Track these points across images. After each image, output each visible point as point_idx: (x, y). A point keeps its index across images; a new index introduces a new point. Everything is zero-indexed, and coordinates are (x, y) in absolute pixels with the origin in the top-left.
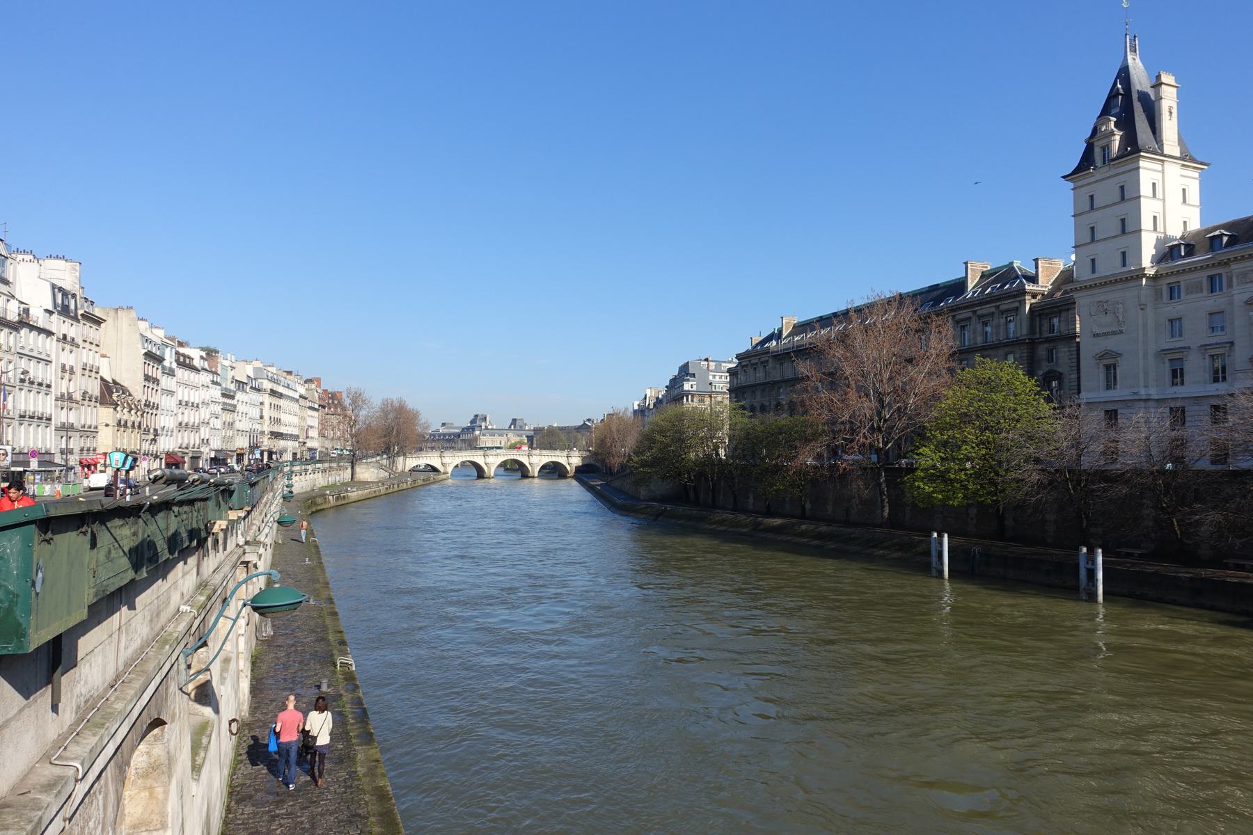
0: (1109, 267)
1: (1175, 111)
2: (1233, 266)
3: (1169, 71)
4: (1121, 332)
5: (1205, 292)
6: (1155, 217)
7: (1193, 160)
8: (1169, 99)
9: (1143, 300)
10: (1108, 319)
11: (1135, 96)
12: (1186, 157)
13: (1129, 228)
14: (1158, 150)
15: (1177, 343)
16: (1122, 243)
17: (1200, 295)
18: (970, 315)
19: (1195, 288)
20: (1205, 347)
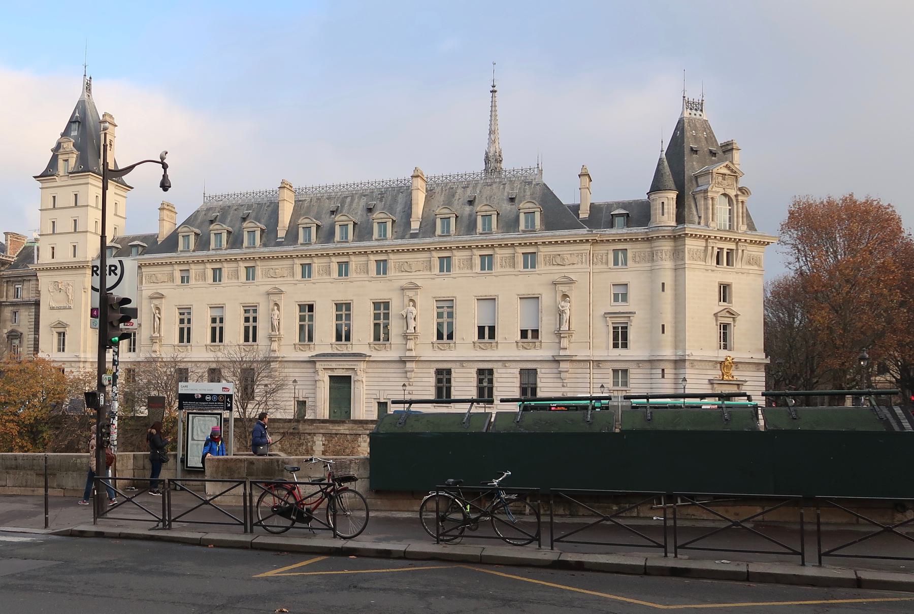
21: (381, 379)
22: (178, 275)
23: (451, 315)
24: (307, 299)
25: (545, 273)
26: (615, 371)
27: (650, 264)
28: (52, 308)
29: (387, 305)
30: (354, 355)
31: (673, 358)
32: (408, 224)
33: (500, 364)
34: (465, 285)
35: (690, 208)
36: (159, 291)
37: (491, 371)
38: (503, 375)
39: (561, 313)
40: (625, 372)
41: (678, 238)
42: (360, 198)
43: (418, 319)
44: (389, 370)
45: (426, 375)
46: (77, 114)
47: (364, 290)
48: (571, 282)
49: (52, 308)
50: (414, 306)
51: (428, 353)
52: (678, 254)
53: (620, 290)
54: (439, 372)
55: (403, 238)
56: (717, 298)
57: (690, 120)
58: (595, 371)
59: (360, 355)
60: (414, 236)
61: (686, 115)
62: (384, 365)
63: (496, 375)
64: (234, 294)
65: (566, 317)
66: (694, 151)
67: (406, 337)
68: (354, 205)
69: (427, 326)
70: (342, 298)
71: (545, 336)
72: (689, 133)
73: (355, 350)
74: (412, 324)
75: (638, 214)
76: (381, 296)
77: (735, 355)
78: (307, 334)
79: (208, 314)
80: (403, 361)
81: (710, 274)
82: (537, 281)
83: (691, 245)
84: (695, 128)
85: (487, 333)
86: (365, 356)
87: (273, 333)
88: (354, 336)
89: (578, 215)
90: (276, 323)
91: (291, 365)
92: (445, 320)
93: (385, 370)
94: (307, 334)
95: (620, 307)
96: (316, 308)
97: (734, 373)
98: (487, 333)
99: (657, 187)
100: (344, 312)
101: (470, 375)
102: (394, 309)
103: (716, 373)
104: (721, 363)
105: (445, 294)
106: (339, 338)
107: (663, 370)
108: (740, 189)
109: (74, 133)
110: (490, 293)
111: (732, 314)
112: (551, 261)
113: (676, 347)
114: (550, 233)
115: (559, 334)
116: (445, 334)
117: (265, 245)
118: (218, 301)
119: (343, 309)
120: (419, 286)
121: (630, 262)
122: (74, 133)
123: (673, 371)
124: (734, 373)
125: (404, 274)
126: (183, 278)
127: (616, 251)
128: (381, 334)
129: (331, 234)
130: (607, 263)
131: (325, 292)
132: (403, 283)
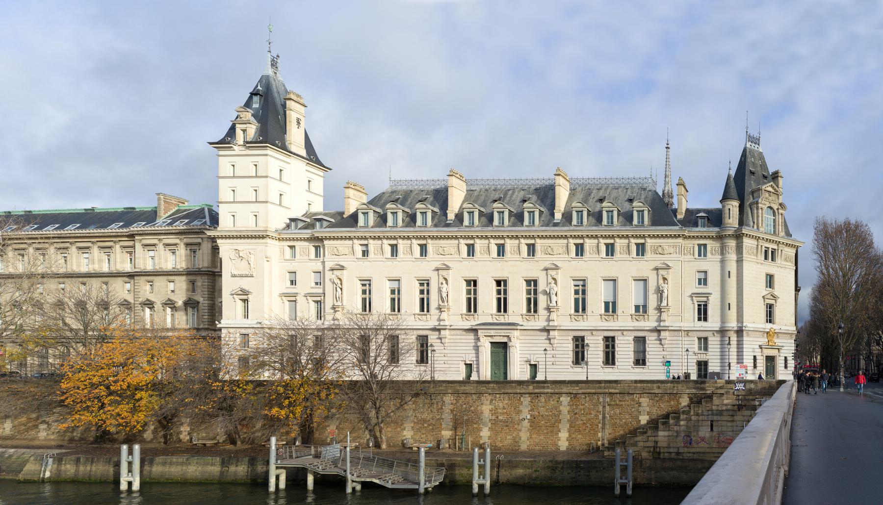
22: (359, 250)
23: (584, 292)
24: (471, 276)
26: (699, 339)
29: (535, 282)
30: (509, 324)
32: (553, 215)
33: (620, 333)
34: (594, 267)
35: (748, 215)
37: (613, 338)
40: (706, 339)
43: (559, 294)
46: (259, 87)
47: (517, 268)
53: (702, 276)
55: (547, 225)
56: (765, 284)
57: (751, 150)
58: (686, 339)
59: (513, 324)
60: (556, 225)
61: (748, 145)
64: (410, 267)
66: (753, 173)
72: (750, 159)
74: (554, 298)
75: (715, 218)
76: (532, 275)
77: (775, 327)
79: (388, 286)
83: (747, 242)
84: (754, 157)
85: (611, 308)
86: (518, 324)
89: (676, 217)
90: (444, 295)
92: (580, 296)
96: (479, 284)
97: (776, 340)
98: (611, 308)
99: (725, 198)
100: (502, 288)
102: (541, 286)
104: (768, 333)
105: (580, 274)
108: (780, 204)
109: (256, 105)
113: (738, 321)
116: (581, 306)
117: (436, 226)
120: (562, 266)
122: (256, 105)
126: (364, 252)
129: (490, 219)
132: (547, 264)
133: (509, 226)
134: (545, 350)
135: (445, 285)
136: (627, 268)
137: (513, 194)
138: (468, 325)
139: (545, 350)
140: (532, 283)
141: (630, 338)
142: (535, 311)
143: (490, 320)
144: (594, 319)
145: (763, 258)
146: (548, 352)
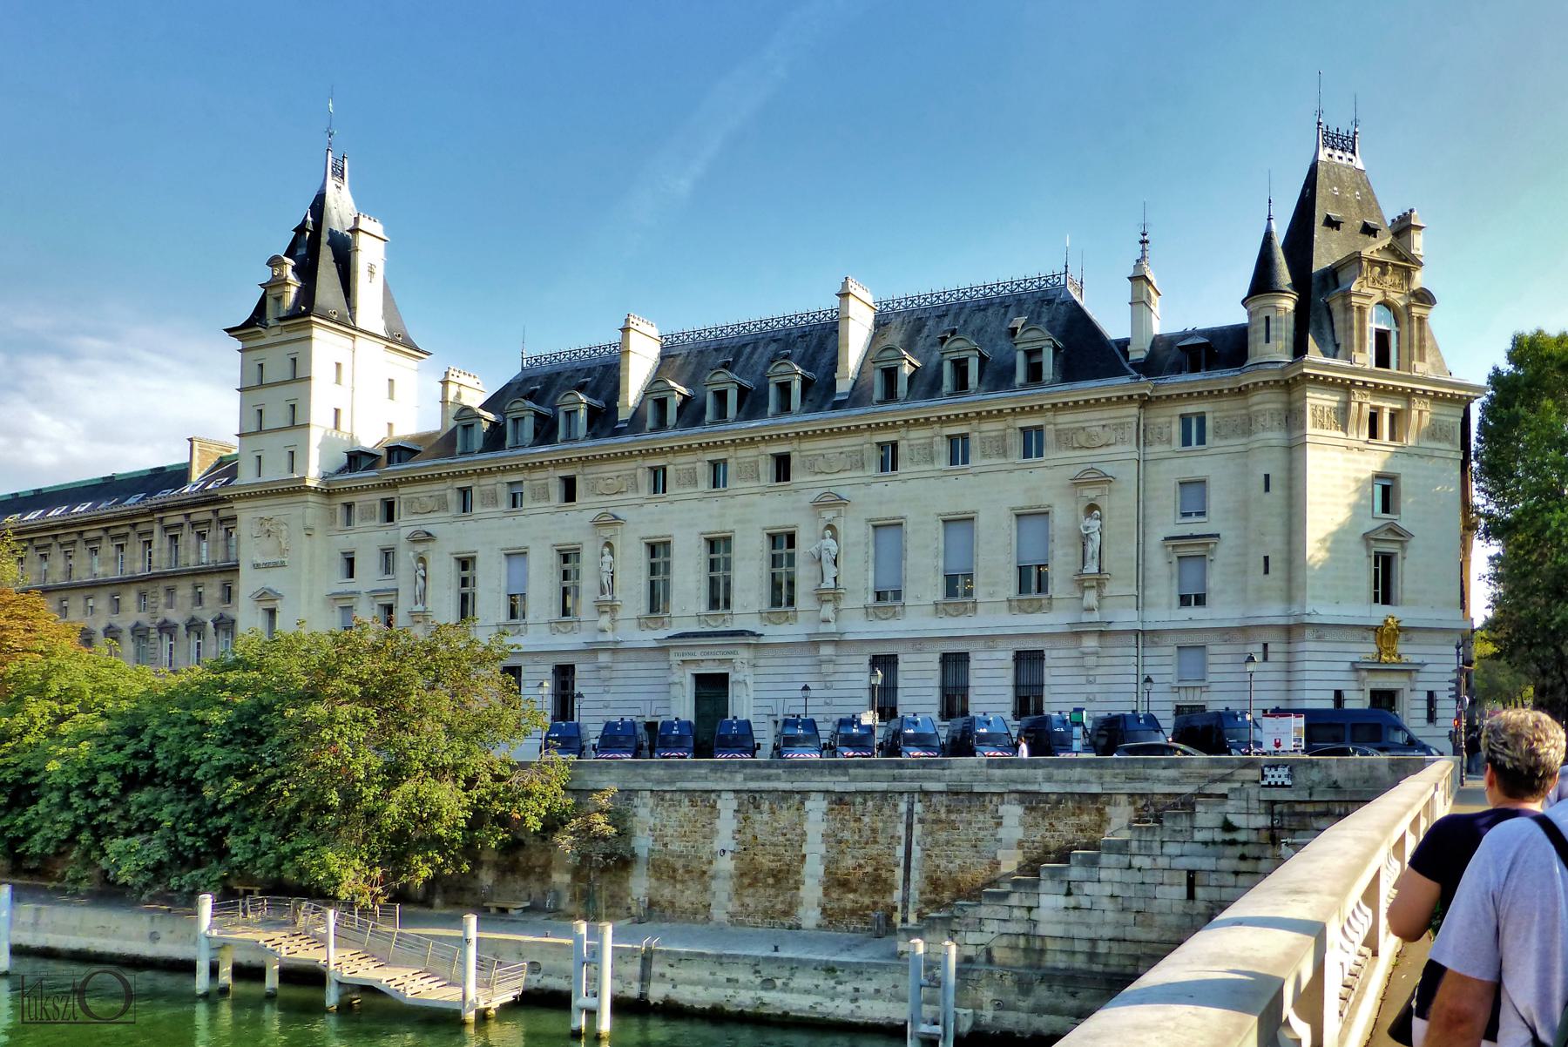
0: (275, 472)
1: (380, 271)
2: (402, 490)
3: (374, 217)
4: (283, 565)
5: (377, 522)
6: (337, 411)
7: (409, 344)
8: (370, 253)
9: (309, 523)
10: (269, 544)
11: (325, 238)
12: (398, 339)
13: (297, 422)
14: (346, 321)
15: (350, 586)
16: (289, 438)
17: (373, 523)
18: (180, 519)
19: (368, 515)
20: (375, 594)
21: (779, 678)
25: (1059, 463)
27: (1244, 440)
28: (257, 566)
29: (791, 539)
31: (1282, 621)
33: (980, 644)
36: (428, 529)
38: (986, 664)
39: (1085, 539)
41: (1292, 385)
42: (768, 344)
43: (841, 562)
44: (792, 661)
45: (855, 668)
48: (1107, 480)
49: (257, 566)
50: (835, 537)
51: (859, 626)
52: (1293, 418)
54: (878, 662)
59: (741, 633)
62: (785, 651)
63: (973, 664)
65: (1092, 548)
67: (821, 597)
68: (755, 356)
69: (859, 578)
70: (715, 528)
71: (1059, 584)
73: (736, 626)
74: (830, 571)
78: (657, 599)
80: (814, 644)
81: (1355, 455)
82: (1044, 481)
86: (753, 634)
87: (602, 598)
88: (736, 599)
91: (633, 655)
93: (785, 662)
94: (657, 599)
95: (1194, 526)
101: (929, 666)
103: (1369, 649)
106: (714, 603)
107: (1265, 645)
110: (965, 506)
111: (1398, 534)
112: (1067, 439)
114: (1066, 387)
115: (1082, 582)
118: (516, 543)
119: (717, 545)
121: (1209, 437)
123: (1283, 647)
124: (1400, 649)
125: (819, 477)
127: (1185, 419)
128: (782, 593)
130: (1169, 441)
131: (686, 518)
133: (737, 419)
134: (806, 688)
135: (608, 558)
136: (996, 489)
137: (752, 353)
138: (649, 637)
139: (806, 688)
140: (783, 541)
141: (1005, 656)
142: (791, 602)
143: (695, 628)
144: (921, 619)
145: (1365, 435)
146: (813, 693)
